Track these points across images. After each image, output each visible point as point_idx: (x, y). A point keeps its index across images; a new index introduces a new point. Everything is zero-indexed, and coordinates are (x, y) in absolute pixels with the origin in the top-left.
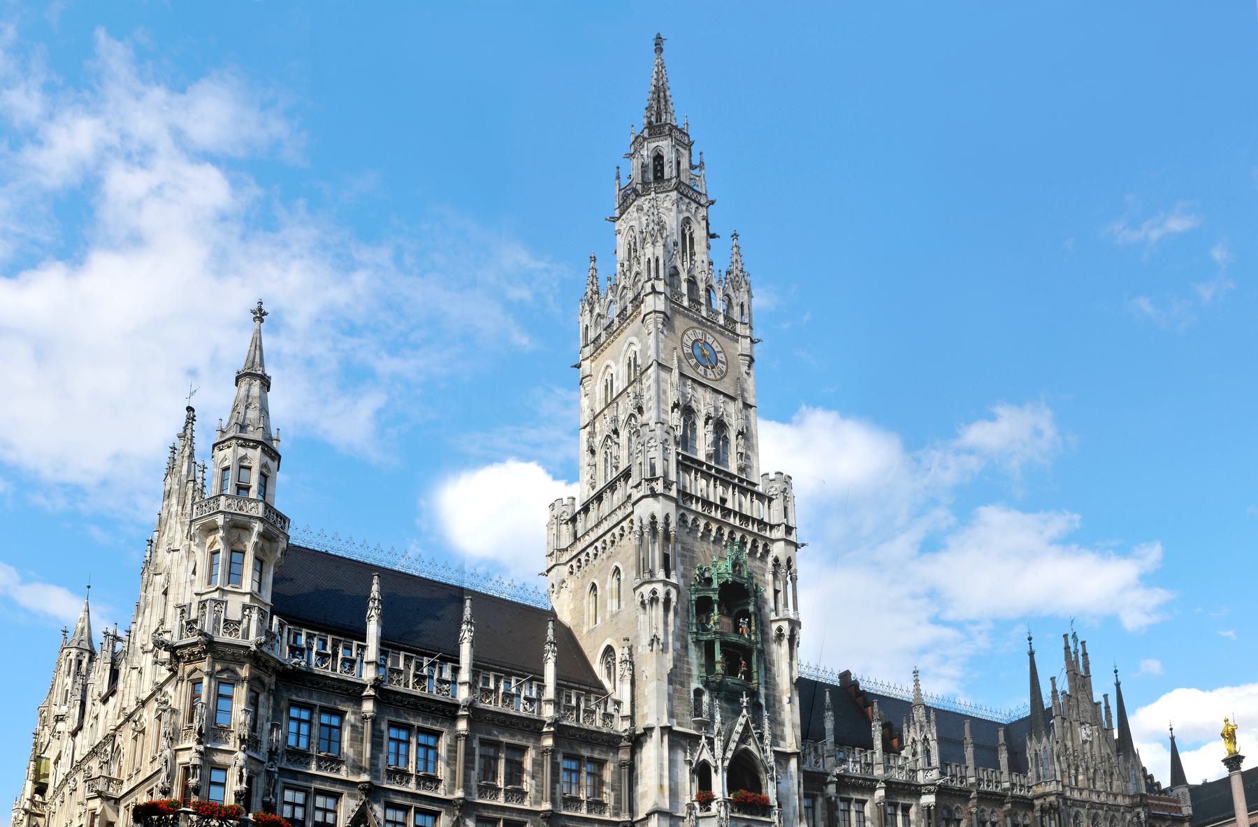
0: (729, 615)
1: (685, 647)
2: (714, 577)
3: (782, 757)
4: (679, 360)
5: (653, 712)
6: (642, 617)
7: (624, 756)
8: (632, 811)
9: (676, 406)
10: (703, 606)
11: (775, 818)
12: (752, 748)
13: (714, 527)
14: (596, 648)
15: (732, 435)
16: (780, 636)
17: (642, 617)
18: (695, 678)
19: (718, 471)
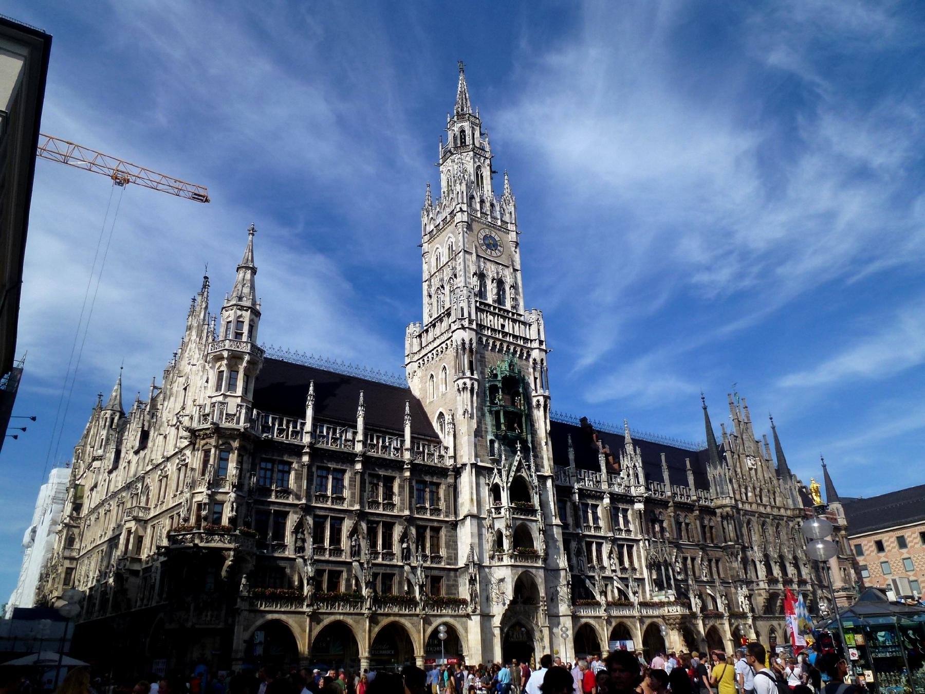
0: (508, 394)
1: (483, 415)
2: (499, 373)
3: (542, 479)
4: (476, 248)
5: (466, 455)
6: (458, 398)
7: (451, 480)
8: (456, 514)
9: (475, 274)
10: (494, 390)
11: (539, 517)
12: (524, 474)
13: (498, 343)
14: (434, 413)
15: (507, 288)
16: (538, 405)
17: (458, 398)
18: (490, 433)
19: (500, 310)
